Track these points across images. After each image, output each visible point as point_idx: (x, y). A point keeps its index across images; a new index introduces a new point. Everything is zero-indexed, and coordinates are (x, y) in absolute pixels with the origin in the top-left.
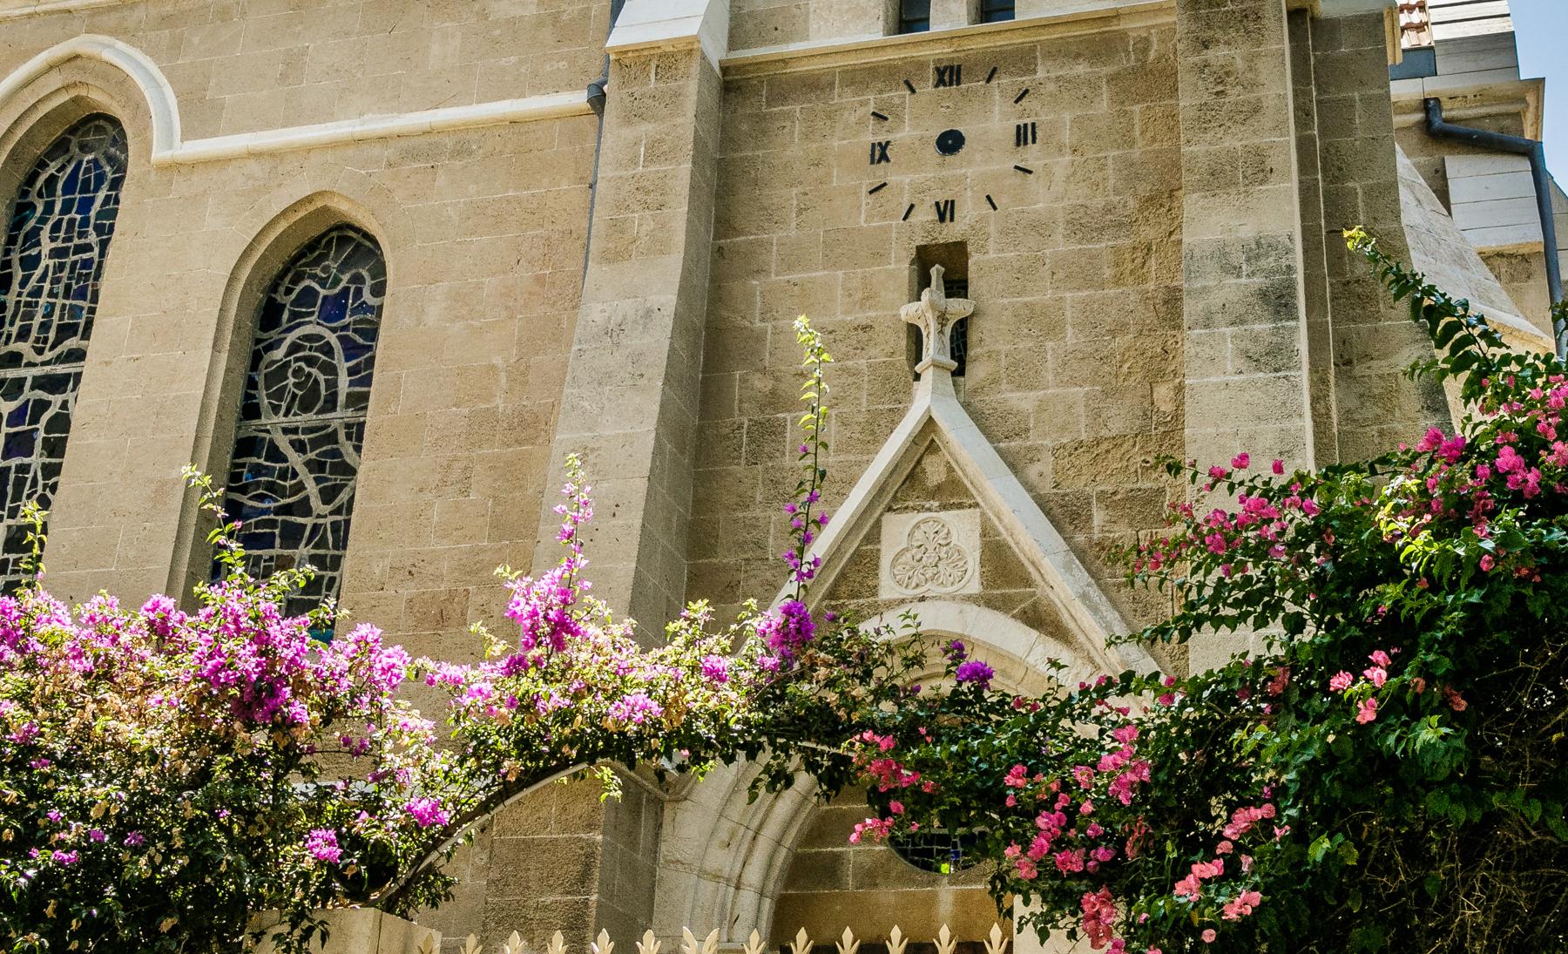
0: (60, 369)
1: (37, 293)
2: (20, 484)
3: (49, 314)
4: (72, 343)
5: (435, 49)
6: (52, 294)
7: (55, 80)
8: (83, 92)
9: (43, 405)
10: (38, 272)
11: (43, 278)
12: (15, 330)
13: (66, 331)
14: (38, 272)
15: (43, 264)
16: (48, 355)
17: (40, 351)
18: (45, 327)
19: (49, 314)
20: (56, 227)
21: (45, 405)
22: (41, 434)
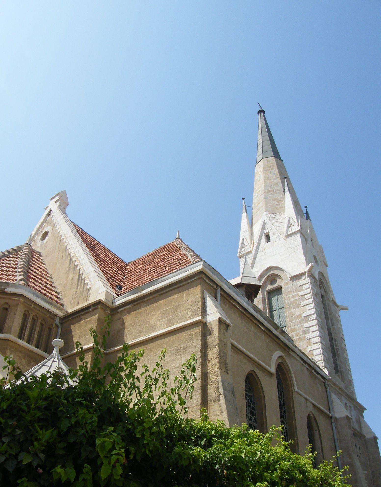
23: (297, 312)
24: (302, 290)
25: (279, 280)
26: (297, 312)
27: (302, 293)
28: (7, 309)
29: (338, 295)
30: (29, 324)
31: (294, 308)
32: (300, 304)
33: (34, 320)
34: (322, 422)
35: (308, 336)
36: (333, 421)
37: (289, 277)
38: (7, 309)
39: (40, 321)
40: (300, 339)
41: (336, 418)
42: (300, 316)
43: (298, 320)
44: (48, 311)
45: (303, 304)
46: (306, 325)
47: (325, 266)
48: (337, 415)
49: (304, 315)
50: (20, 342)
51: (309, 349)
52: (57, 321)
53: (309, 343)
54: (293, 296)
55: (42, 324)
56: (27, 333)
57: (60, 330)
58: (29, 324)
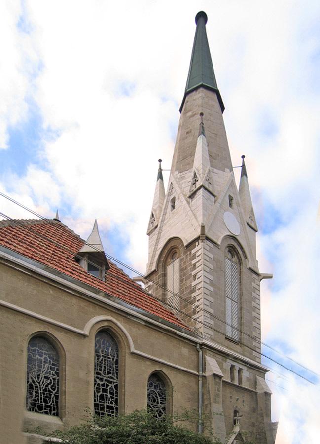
0: (111, 380)
1: (101, 362)
2: (107, 398)
3: (105, 367)
4: (111, 375)
5: (175, 354)
6: (105, 364)
7: (106, 324)
8: (111, 328)
9: (107, 386)
10: (101, 359)
11: (102, 360)
12: (98, 368)
13: (109, 373)
14: (101, 359)
15: (101, 357)
16: (107, 376)
17: (105, 375)
18: (105, 370)
19: (105, 367)
20: (102, 351)
21: (109, 385)
22: (109, 391)
48: (206, 375)
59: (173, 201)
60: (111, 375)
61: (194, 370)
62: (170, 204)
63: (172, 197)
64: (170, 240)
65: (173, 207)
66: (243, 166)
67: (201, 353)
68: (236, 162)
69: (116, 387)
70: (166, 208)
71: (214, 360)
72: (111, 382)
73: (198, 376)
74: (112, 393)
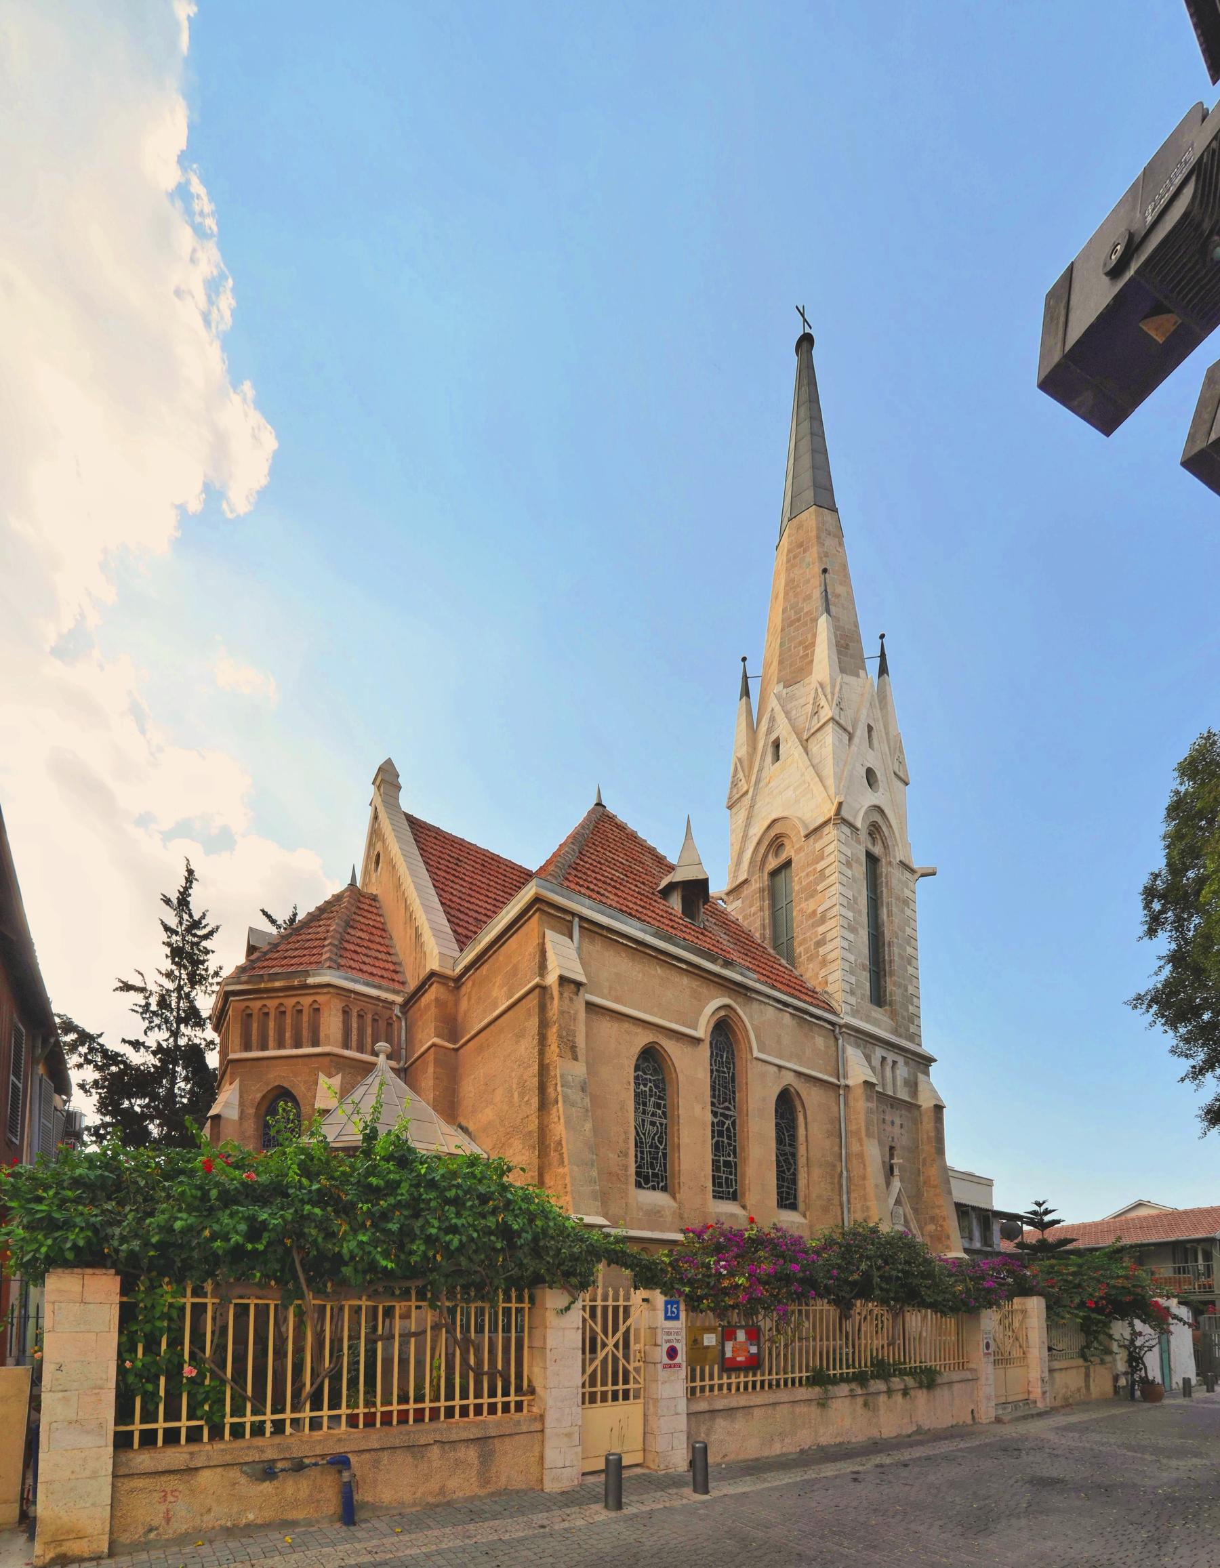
4: (727, 1104)
23: (810, 906)
24: (822, 858)
25: (788, 846)
26: (810, 906)
27: (820, 866)
28: (318, 1009)
29: (916, 841)
30: (355, 1025)
31: (806, 900)
32: (815, 890)
33: (360, 1016)
34: (812, 1098)
35: (822, 951)
36: (841, 1092)
37: (803, 833)
38: (318, 1009)
39: (370, 1016)
40: (810, 959)
41: (847, 1086)
42: (814, 912)
43: (810, 922)
44: (378, 999)
45: (820, 888)
46: (821, 929)
47: (901, 785)
48: (850, 1082)
49: (820, 910)
50: (347, 1053)
51: (822, 973)
52: (397, 1011)
53: (824, 963)
54: (807, 875)
55: (374, 1020)
56: (354, 1037)
57: (403, 1024)
58: (355, 1025)
59: (777, 745)
60: (727, 1104)
61: (831, 1076)
62: (770, 751)
63: (773, 737)
64: (774, 821)
65: (777, 757)
66: (883, 655)
67: (840, 1041)
68: (870, 649)
69: (734, 1123)
70: (763, 759)
71: (859, 1053)
72: (726, 1116)
73: (839, 1086)
74: (729, 1138)
